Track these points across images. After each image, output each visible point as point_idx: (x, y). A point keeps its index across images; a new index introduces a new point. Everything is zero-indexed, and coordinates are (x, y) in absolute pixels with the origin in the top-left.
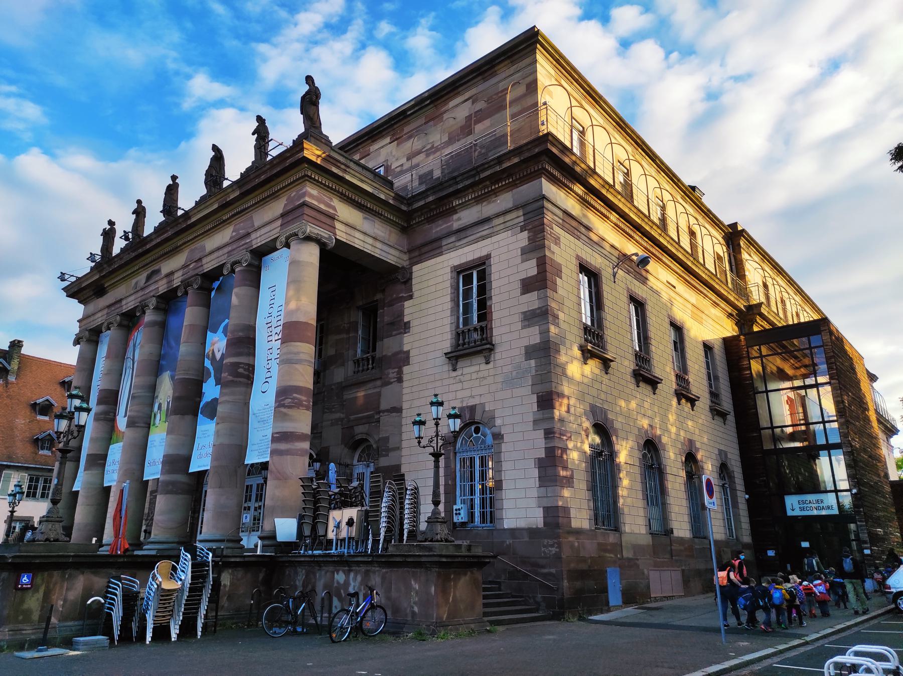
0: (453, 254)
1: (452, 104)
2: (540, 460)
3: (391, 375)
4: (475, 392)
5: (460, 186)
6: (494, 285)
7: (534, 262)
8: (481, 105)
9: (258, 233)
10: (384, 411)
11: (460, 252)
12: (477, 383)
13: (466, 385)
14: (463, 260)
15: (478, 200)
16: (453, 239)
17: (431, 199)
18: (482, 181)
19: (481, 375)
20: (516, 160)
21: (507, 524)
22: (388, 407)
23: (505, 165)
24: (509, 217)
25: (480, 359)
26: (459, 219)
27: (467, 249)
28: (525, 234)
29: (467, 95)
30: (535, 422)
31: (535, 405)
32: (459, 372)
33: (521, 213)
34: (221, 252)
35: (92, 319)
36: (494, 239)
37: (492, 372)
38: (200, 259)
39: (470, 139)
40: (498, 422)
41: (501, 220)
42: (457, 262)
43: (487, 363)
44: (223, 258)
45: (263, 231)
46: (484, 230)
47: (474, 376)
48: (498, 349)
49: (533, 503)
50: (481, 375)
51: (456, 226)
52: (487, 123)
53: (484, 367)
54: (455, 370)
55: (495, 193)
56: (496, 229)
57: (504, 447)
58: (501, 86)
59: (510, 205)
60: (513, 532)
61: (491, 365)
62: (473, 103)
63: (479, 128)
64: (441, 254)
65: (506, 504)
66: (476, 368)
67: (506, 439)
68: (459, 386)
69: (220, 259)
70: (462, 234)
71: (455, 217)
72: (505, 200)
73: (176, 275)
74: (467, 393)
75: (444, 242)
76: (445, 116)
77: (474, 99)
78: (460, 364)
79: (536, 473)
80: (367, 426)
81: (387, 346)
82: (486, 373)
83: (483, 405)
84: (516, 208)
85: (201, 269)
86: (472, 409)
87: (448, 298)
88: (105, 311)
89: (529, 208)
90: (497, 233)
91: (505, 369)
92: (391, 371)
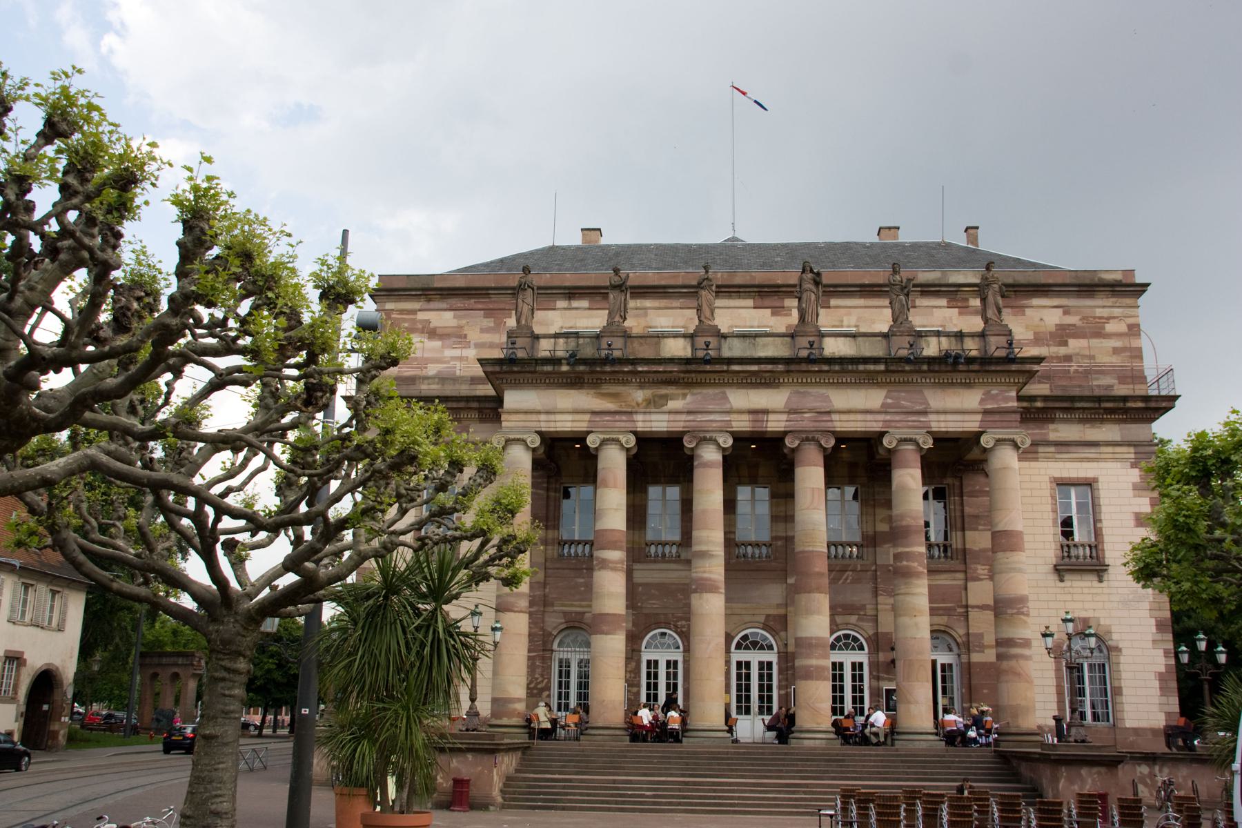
0: (1051, 464)
1: (1036, 301)
2: (1160, 674)
3: (980, 571)
4: (1087, 606)
5: (1078, 405)
6: (1104, 509)
7: (1147, 501)
8: (1072, 320)
9: (942, 417)
10: (973, 607)
11: (1061, 465)
12: (1089, 598)
13: (1076, 597)
14: (1065, 474)
15: (1082, 421)
16: (1052, 449)
17: (1039, 404)
18: (1100, 408)
19: (1094, 591)
20: (1140, 405)
21: (1128, 724)
22: (979, 603)
23: (1129, 405)
24: (1118, 449)
25: (1094, 577)
26: (1056, 430)
27: (1068, 465)
28: (1136, 472)
29: (1056, 302)
30: (1154, 641)
31: (1154, 629)
32: (1067, 584)
33: (1132, 450)
34: (869, 417)
35: (543, 417)
36: (1102, 465)
37: (1106, 591)
38: (829, 413)
39: (1062, 351)
40: (1115, 637)
41: (1110, 449)
42: (1057, 475)
43: (1101, 581)
44: (875, 424)
45: (950, 417)
46: (1090, 452)
47: (1086, 591)
48: (1111, 570)
49: (1156, 708)
50: (1094, 591)
51: (1053, 436)
52: (1083, 343)
53: (1096, 584)
54: (1062, 581)
55: (1102, 421)
56: (1103, 456)
57: (1122, 659)
58: (1099, 312)
59: (1117, 438)
60: (1136, 731)
61: (1104, 584)
62: (1065, 313)
63: (1075, 345)
64: (1036, 459)
65: (1126, 707)
66: (1089, 584)
67: (1124, 652)
68: (1069, 597)
69: (869, 424)
70: (1064, 449)
71: (1051, 426)
72: (1109, 432)
73: (771, 417)
74: (1079, 605)
75: (1041, 449)
76: (1028, 311)
77: (1067, 311)
78: (1067, 577)
79: (1157, 684)
80: (946, 618)
81: (978, 540)
82: (1099, 591)
83: (1098, 619)
84: (1129, 444)
85: (829, 424)
86: (1086, 622)
87: (1049, 508)
88: (587, 417)
89: (1141, 449)
90: (1105, 460)
91: (1120, 591)
92: (979, 567)
